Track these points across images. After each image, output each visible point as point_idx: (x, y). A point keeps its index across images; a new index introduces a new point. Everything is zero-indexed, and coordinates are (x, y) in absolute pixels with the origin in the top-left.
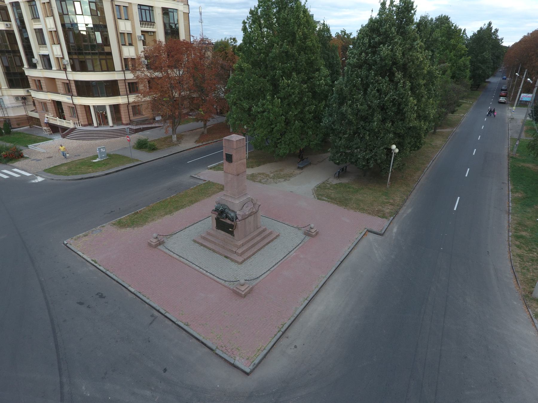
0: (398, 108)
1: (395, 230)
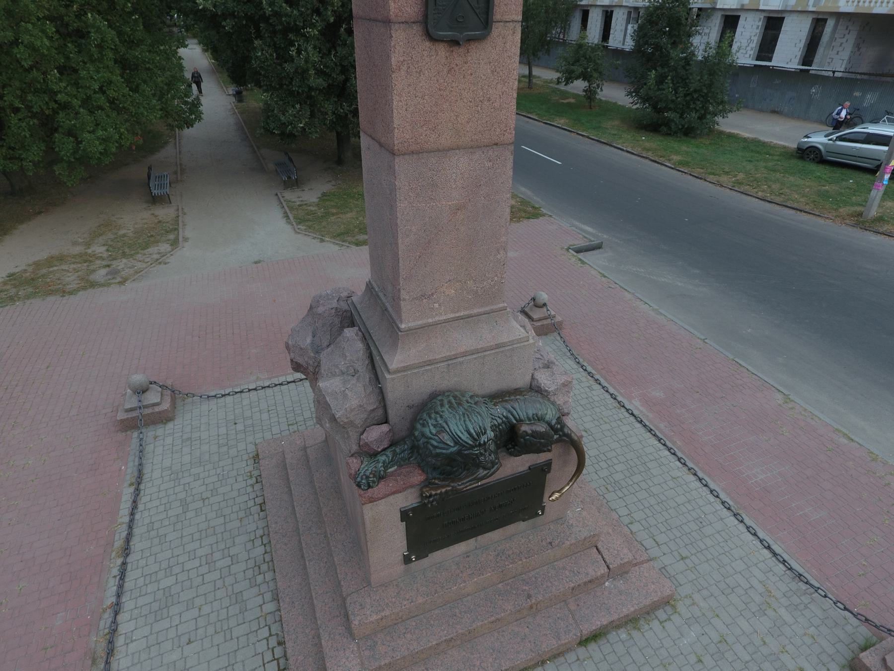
1: (590, 229)
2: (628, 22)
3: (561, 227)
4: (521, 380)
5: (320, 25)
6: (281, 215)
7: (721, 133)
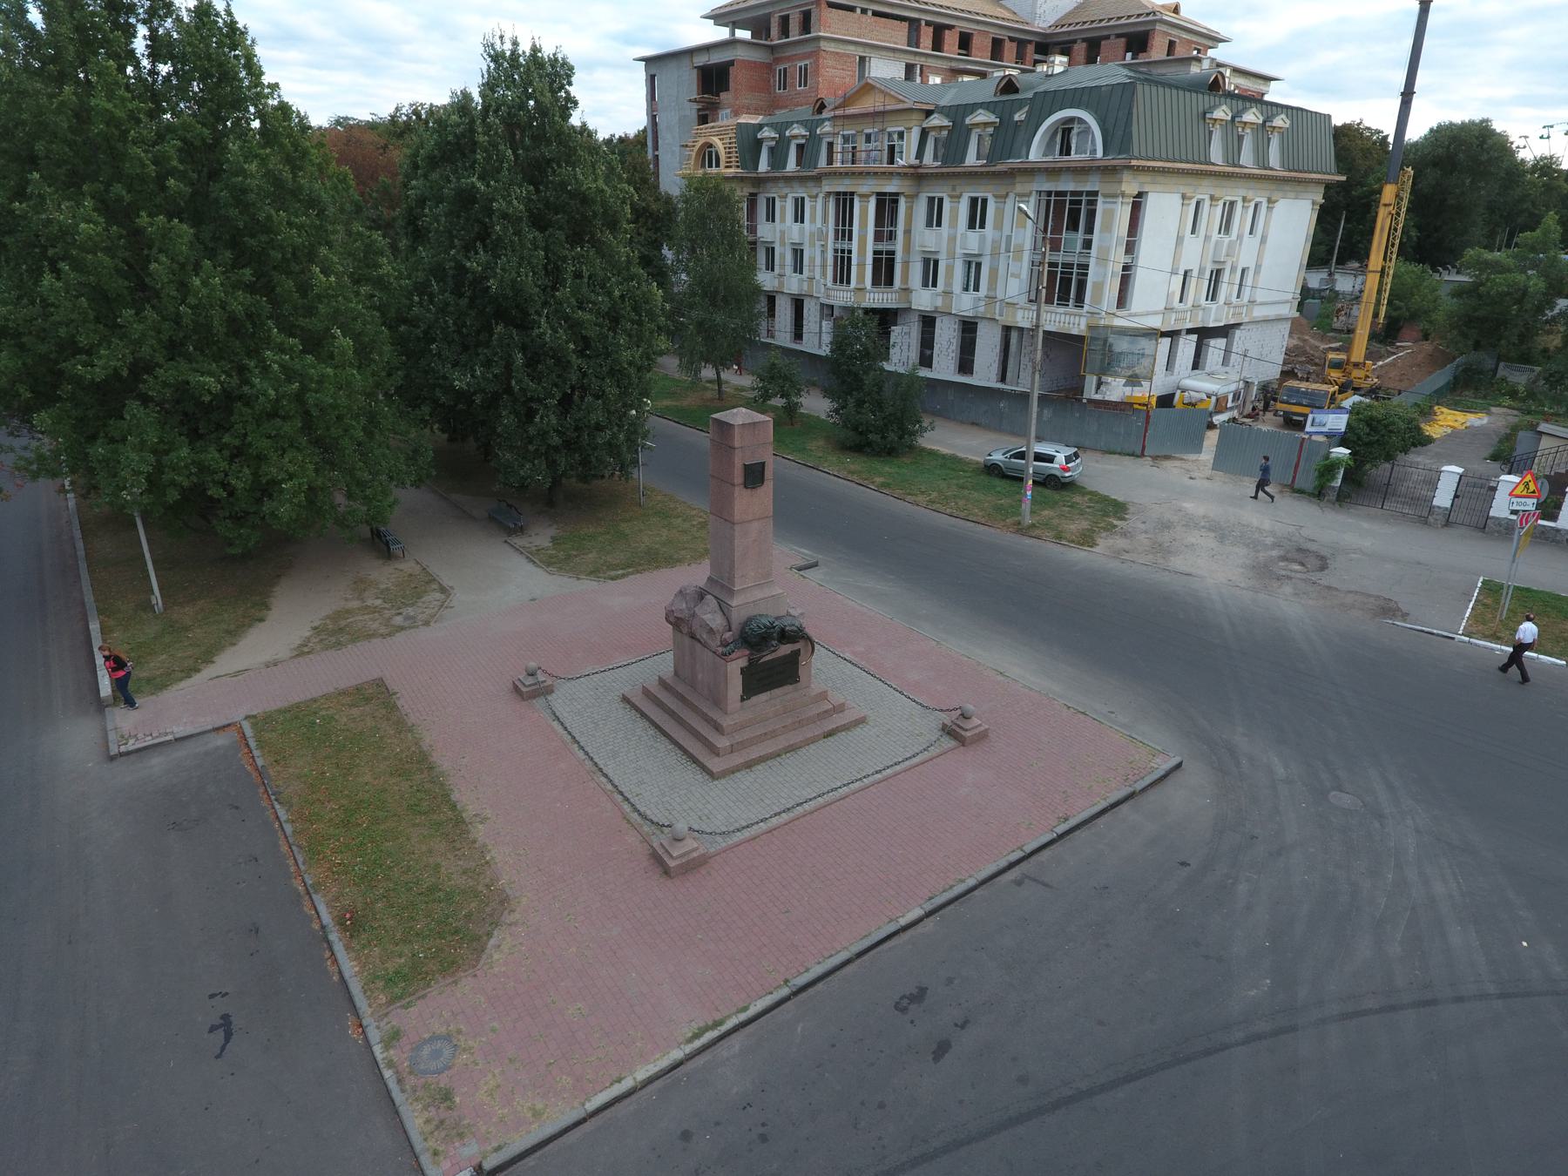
2: (822, 318)
4: (783, 613)
6: (523, 560)
7: (924, 449)
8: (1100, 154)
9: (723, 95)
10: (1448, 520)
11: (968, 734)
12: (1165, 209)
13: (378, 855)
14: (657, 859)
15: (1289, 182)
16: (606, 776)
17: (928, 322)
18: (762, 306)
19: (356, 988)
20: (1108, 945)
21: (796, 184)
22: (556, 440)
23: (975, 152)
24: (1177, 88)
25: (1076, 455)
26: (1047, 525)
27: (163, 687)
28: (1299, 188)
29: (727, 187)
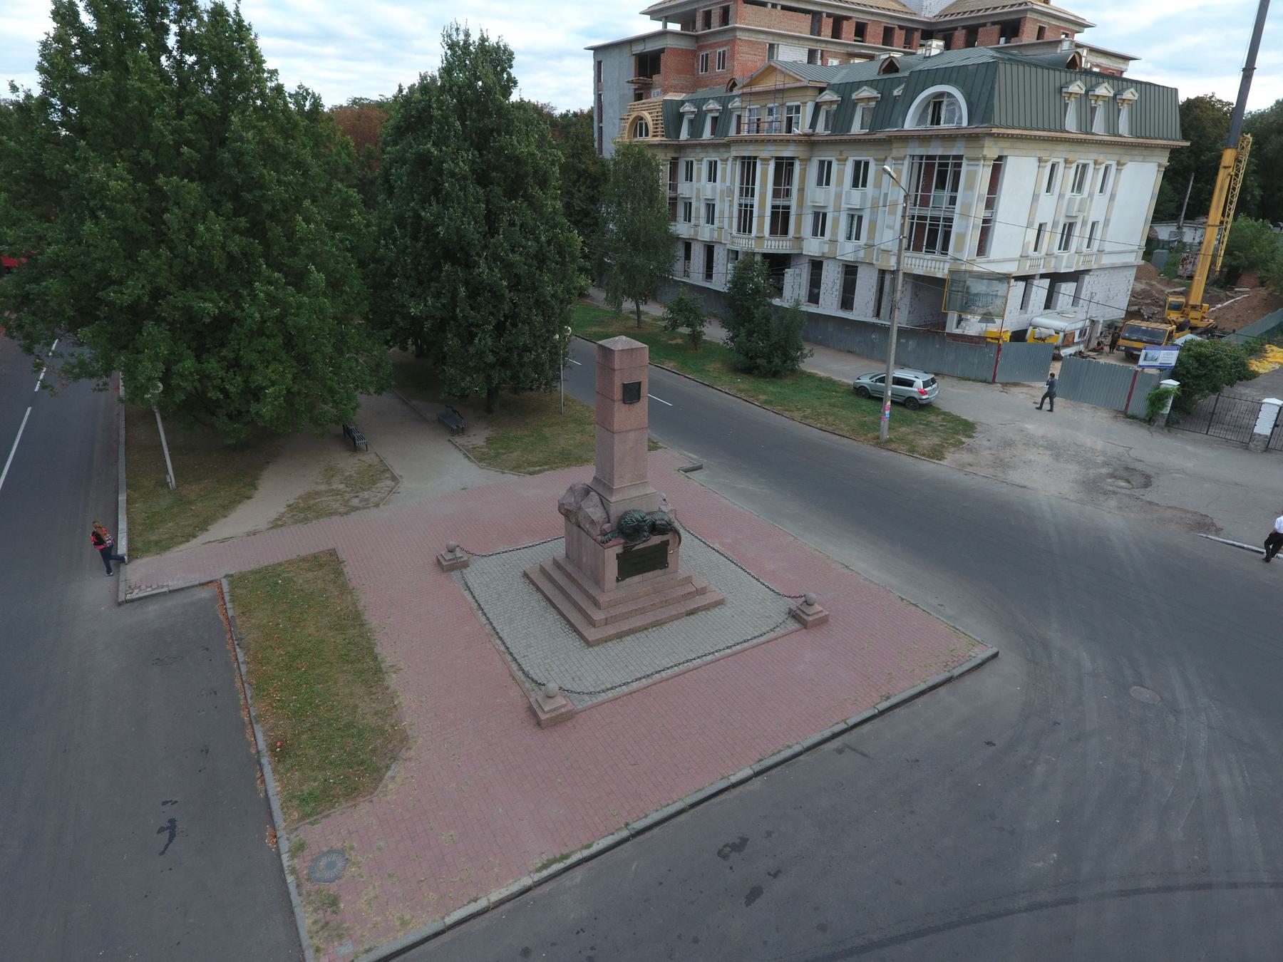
0: (561, 253)
3: (672, 457)
4: (655, 508)
5: (494, 322)
6: (462, 456)
7: (803, 373)
8: (965, 123)
9: (655, 77)
10: (1268, 446)
11: (810, 619)
12: (1022, 171)
13: (309, 694)
14: (532, 712)
15: (1137, 148)
16: (500, 638)
17: (816, 266)
18: (681, 253)
19: (276, 804)
20: (912, 812)
21: (710, 150)
22: (491, 359)
23: (856, 124)
24: (1036, 66)
25: (933, 381)
26: (902, 440)
27: (167, 548)
28: (1145, 153)
29: (649, 153)
